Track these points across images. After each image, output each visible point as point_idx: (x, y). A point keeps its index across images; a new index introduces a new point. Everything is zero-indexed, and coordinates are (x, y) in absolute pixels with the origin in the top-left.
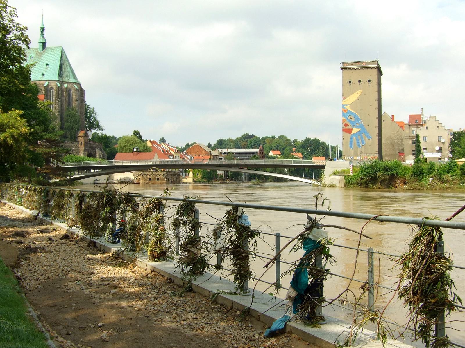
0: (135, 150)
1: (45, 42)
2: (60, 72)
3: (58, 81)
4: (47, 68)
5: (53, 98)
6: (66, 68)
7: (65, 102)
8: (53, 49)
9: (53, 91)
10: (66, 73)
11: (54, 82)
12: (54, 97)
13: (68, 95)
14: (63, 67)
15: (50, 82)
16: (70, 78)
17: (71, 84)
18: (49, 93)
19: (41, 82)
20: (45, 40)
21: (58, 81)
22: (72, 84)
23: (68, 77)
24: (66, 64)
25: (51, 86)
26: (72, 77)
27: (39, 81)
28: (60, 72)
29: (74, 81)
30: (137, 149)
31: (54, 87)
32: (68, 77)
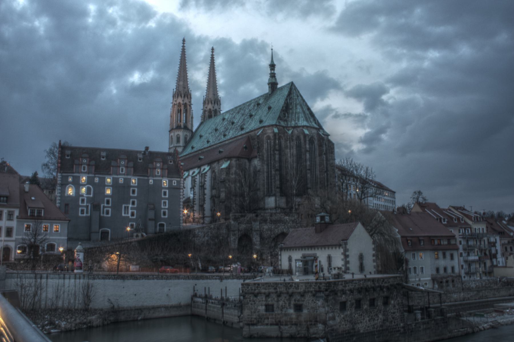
0: (318, 219)
1: (274, 81)
2: (284, 114)
3: (276, 126)
4: (268, 113)
5: (270, 152)
6: (295, 108)
7: (289, 155)
8: (282, 88)
9: (270, 142)
10: (294, 115)
11: (270, 128)
12: (272, 149)
13: (297, 145)
14: (291, 107)
15: (266, 128)
16: (298, 121)
17: (299, 129)
18: (265, 145)
19: (256, 132)
20: (276, 79)
21: (276, 126)
22: (301, 128)
23: (297, 120)
24: (294, 103)
25: (267, 134)
26: (302, 119)
27: (255, 130)
28: (284, 114)
29: (305, 123)
30: (322, 218)
31: (271, 135)
32: (297, 120)
